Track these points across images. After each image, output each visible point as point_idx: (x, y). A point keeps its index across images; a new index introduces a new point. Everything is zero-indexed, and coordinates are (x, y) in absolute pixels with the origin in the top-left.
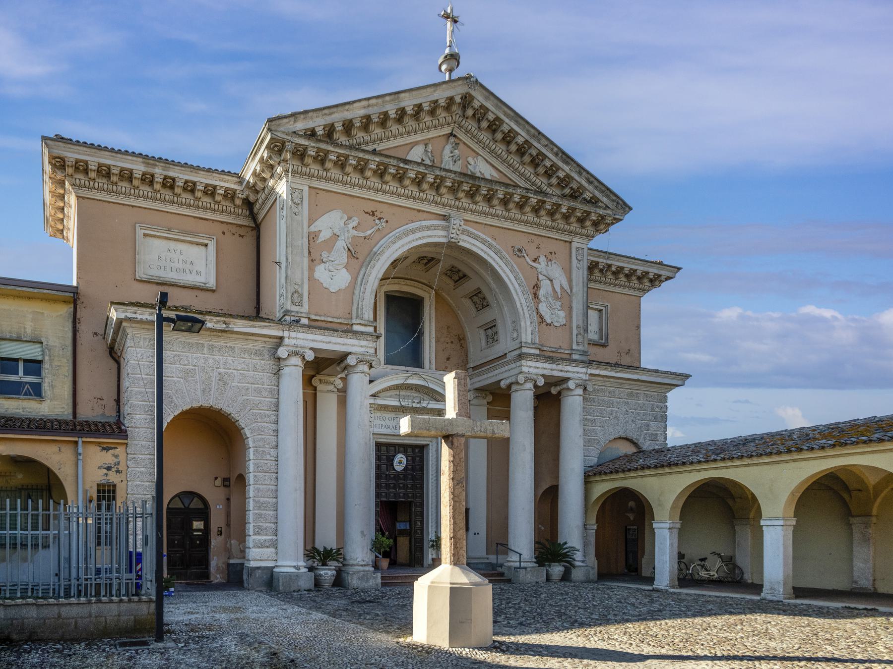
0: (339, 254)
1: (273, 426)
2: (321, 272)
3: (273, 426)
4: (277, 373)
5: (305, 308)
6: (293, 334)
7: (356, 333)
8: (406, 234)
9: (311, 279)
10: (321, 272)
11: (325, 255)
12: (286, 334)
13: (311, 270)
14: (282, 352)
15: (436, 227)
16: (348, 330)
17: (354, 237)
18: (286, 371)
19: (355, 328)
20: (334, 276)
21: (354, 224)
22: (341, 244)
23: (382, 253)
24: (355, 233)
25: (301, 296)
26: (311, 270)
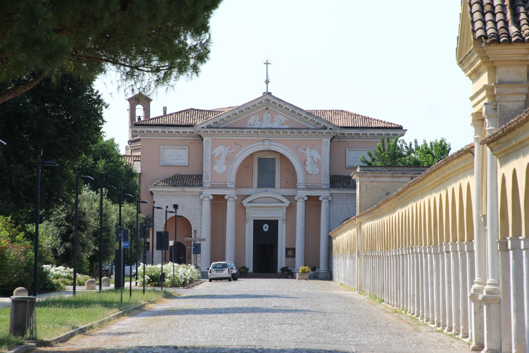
0: (222, 160)
1: (200, 221)
2: (216, 168)
3: (200, 221)
4: (201, 203)
5: (210, 180)
6: (205, 190)
7: (230, 188)
8: (247, 150)
9: (212, 171)
10: (216, 168)
11: (217, 161)
12: (203, 191)
13: (212, 167)
14: (202, 197)
15: (260, 145)
16: (225, 187)
17: (228, 153)
18: (204, 202)
19: (228, 186)
20: (220, 168)
21: (228, 148)
22: (223, 157)
23: (238, 158)
24: (229, 152)
25: (208, 177)
26: (212, 167)
